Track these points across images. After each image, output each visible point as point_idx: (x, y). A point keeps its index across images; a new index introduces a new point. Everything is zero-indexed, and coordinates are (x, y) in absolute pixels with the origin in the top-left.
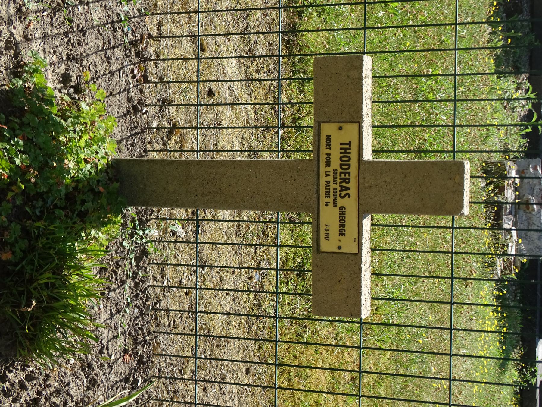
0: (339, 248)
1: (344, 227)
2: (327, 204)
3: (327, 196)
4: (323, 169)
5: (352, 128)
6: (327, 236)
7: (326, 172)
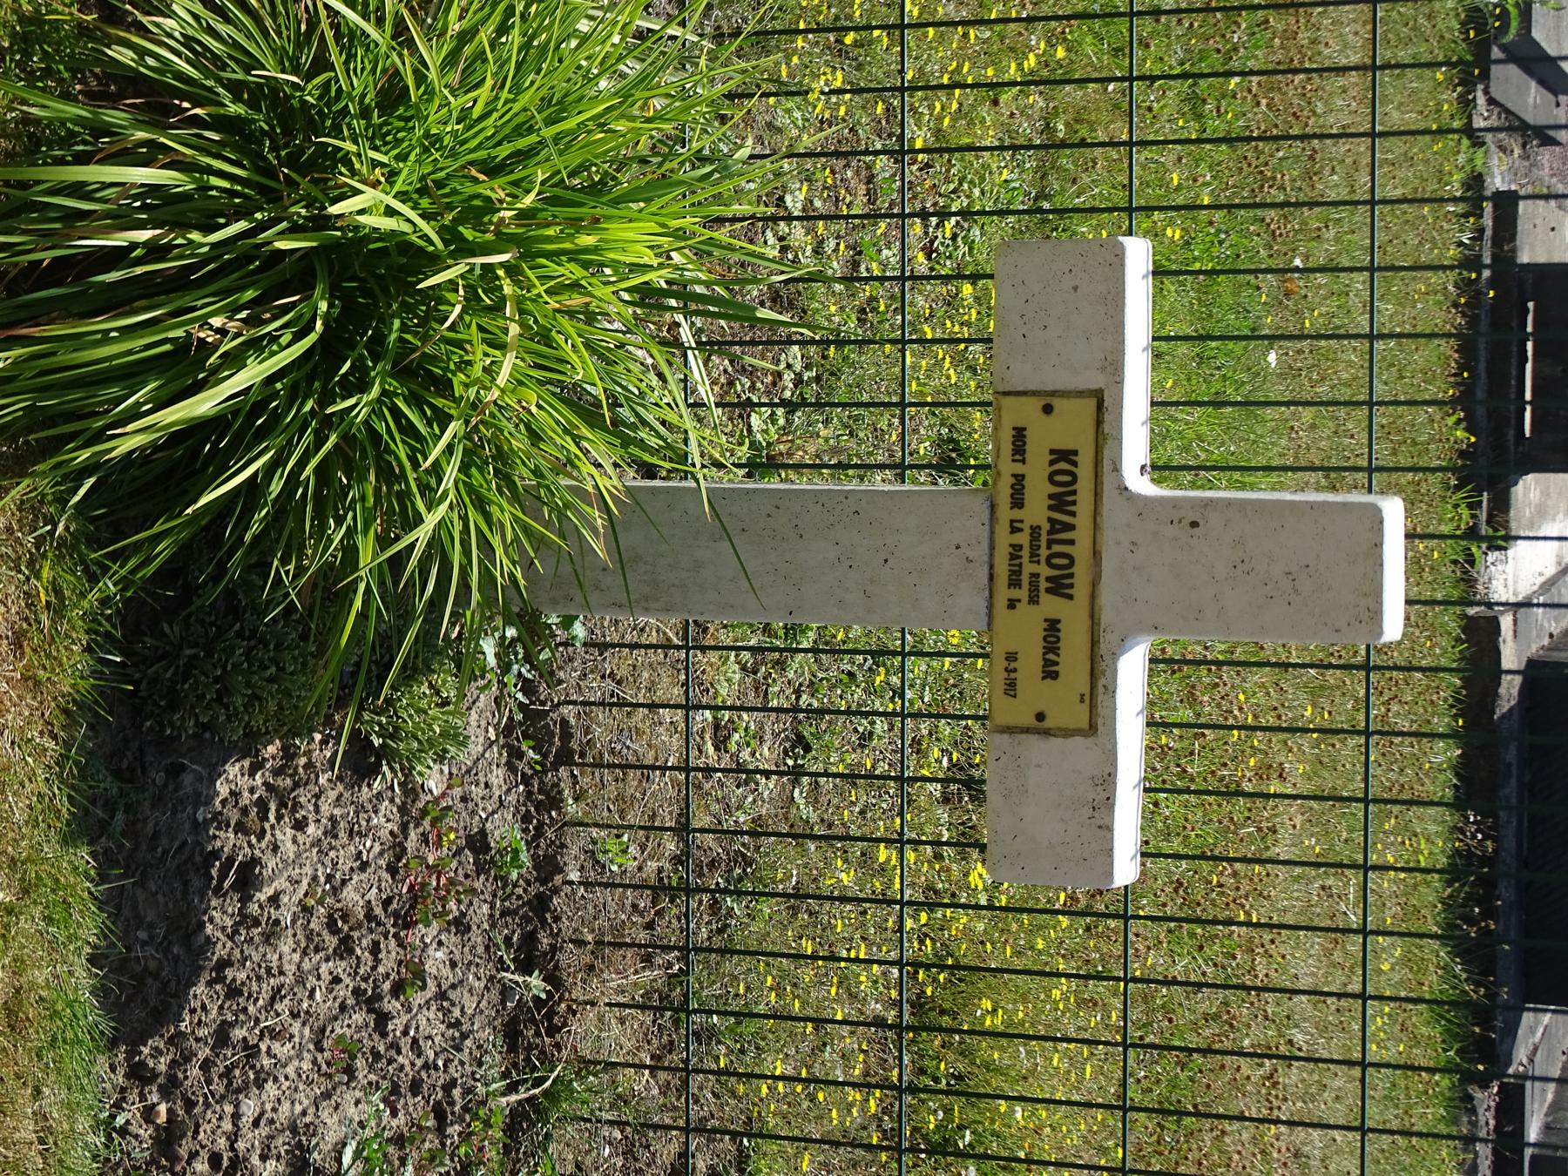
0: (1040, 717)
2: (1012, 604)
3: (1014, 582)
4: (1005, 513)
7: (1012, 521)
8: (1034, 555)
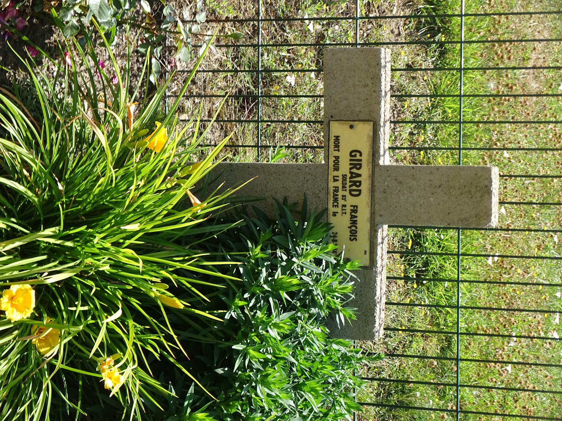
1: (356, 213)
4: (333, 173)
5: (365, 129)
7: (334, 177)
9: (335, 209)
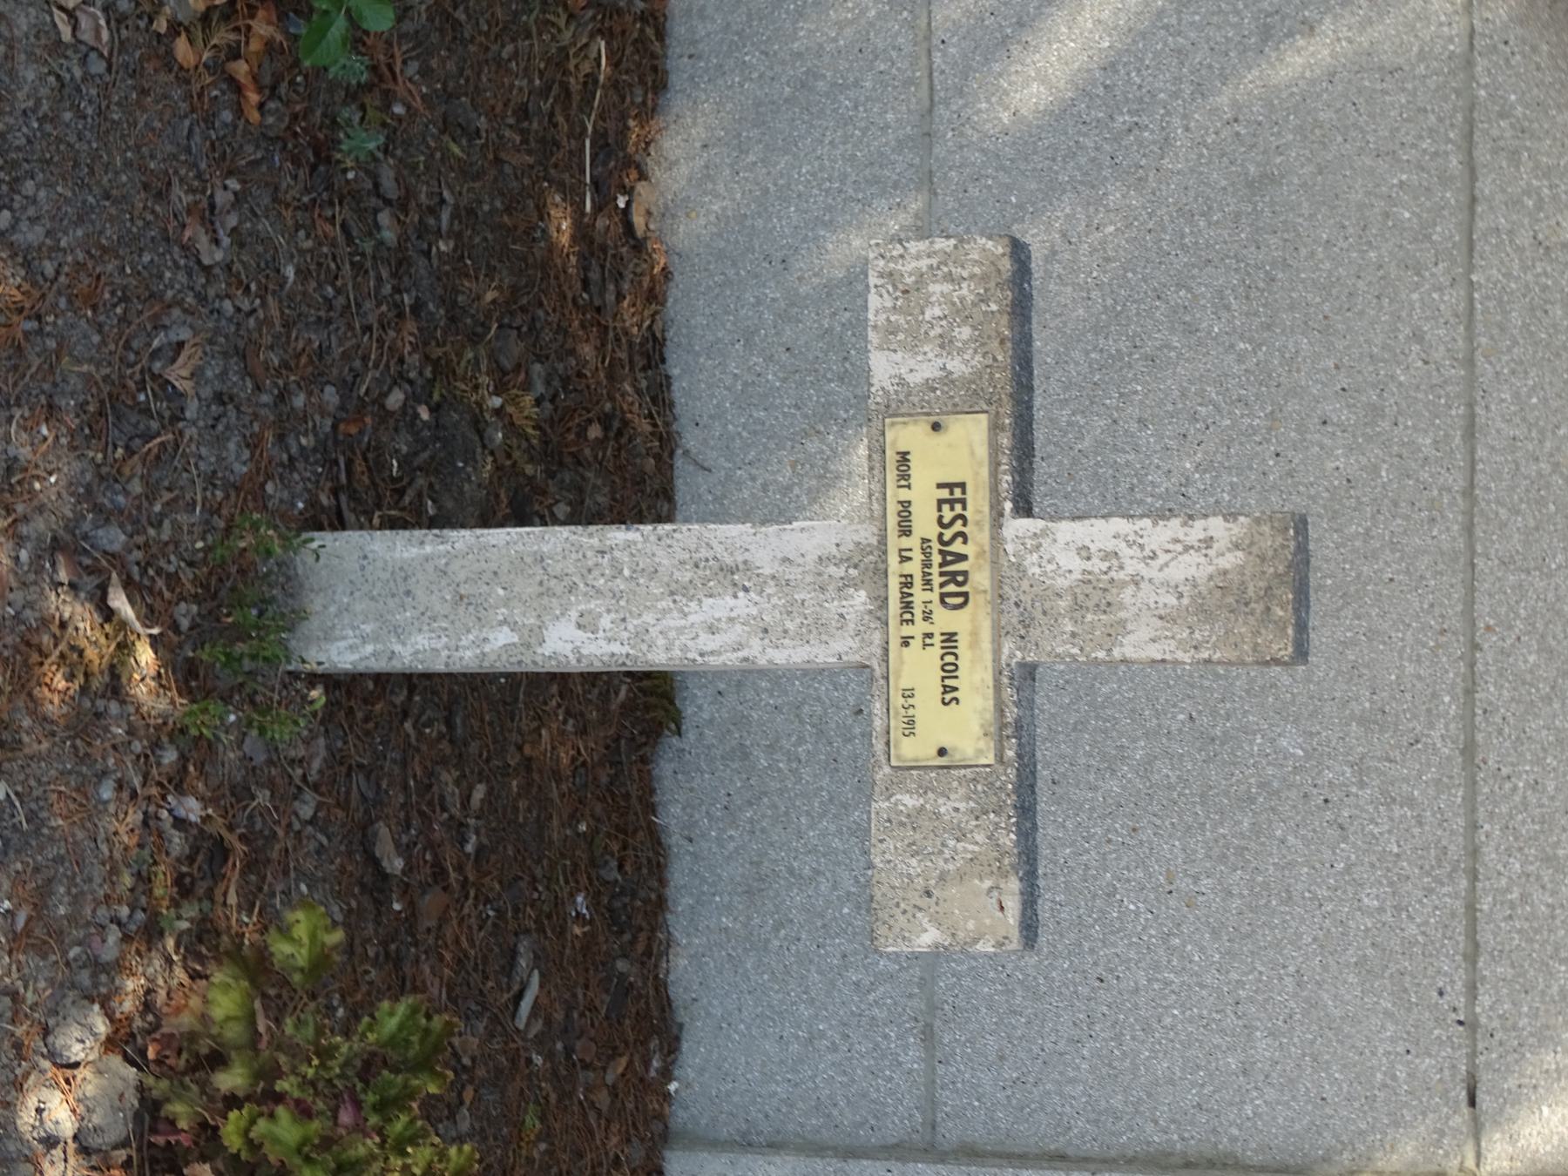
0: (942, 752)
4: (894, 542)
6: (911, 722)
8: (927, 583)
9: (907, 630)
